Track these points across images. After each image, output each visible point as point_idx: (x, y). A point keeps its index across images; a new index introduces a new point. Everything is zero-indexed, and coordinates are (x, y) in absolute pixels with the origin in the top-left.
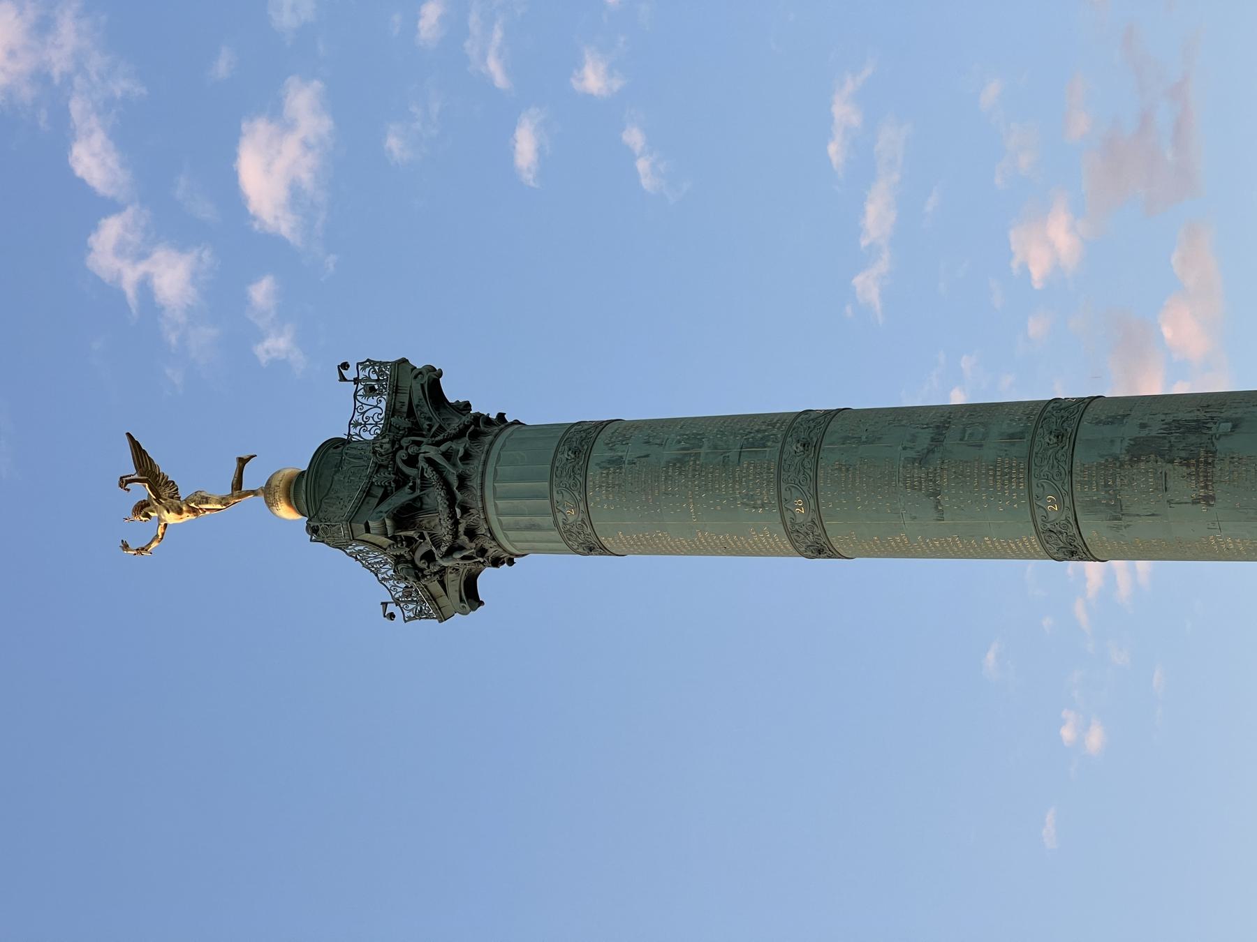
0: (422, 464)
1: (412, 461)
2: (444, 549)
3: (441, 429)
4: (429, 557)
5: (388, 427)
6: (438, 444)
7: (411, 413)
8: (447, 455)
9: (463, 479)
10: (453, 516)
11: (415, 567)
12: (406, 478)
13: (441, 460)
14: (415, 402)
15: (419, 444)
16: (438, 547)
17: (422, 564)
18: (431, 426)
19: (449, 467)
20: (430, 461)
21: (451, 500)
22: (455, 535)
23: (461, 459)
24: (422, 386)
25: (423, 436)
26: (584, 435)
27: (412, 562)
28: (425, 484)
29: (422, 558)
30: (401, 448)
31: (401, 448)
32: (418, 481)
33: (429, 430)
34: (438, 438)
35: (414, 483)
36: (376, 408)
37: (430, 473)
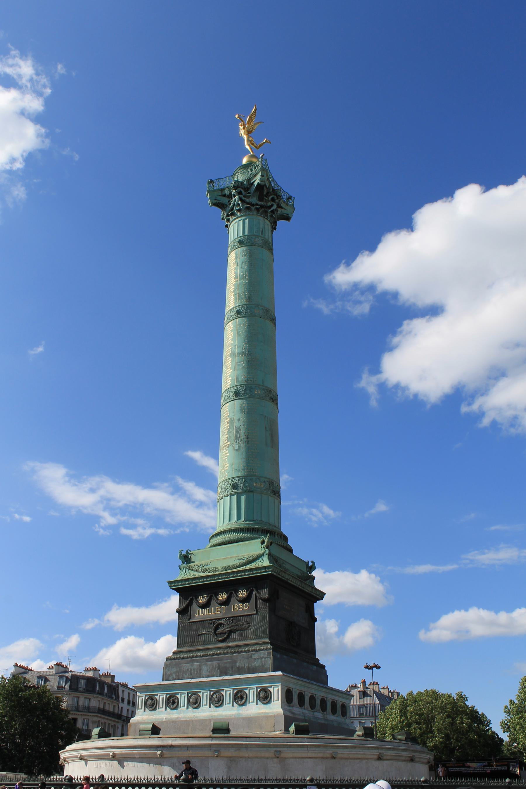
0: (272, 203)
1: (273, 200)
2: (243, 198)
8: (273, 212)
10: (257, 204)
13: (272, 209)
14: (283, 210)
16: (244, 196)
17: (238, 190)
19: (270, 210)
20: (272, 205)
22: (248, 204)
27: (239, 187)
28: (267, 201)
30: (278, 198)
36: (284, 197)
37: (269, 204)
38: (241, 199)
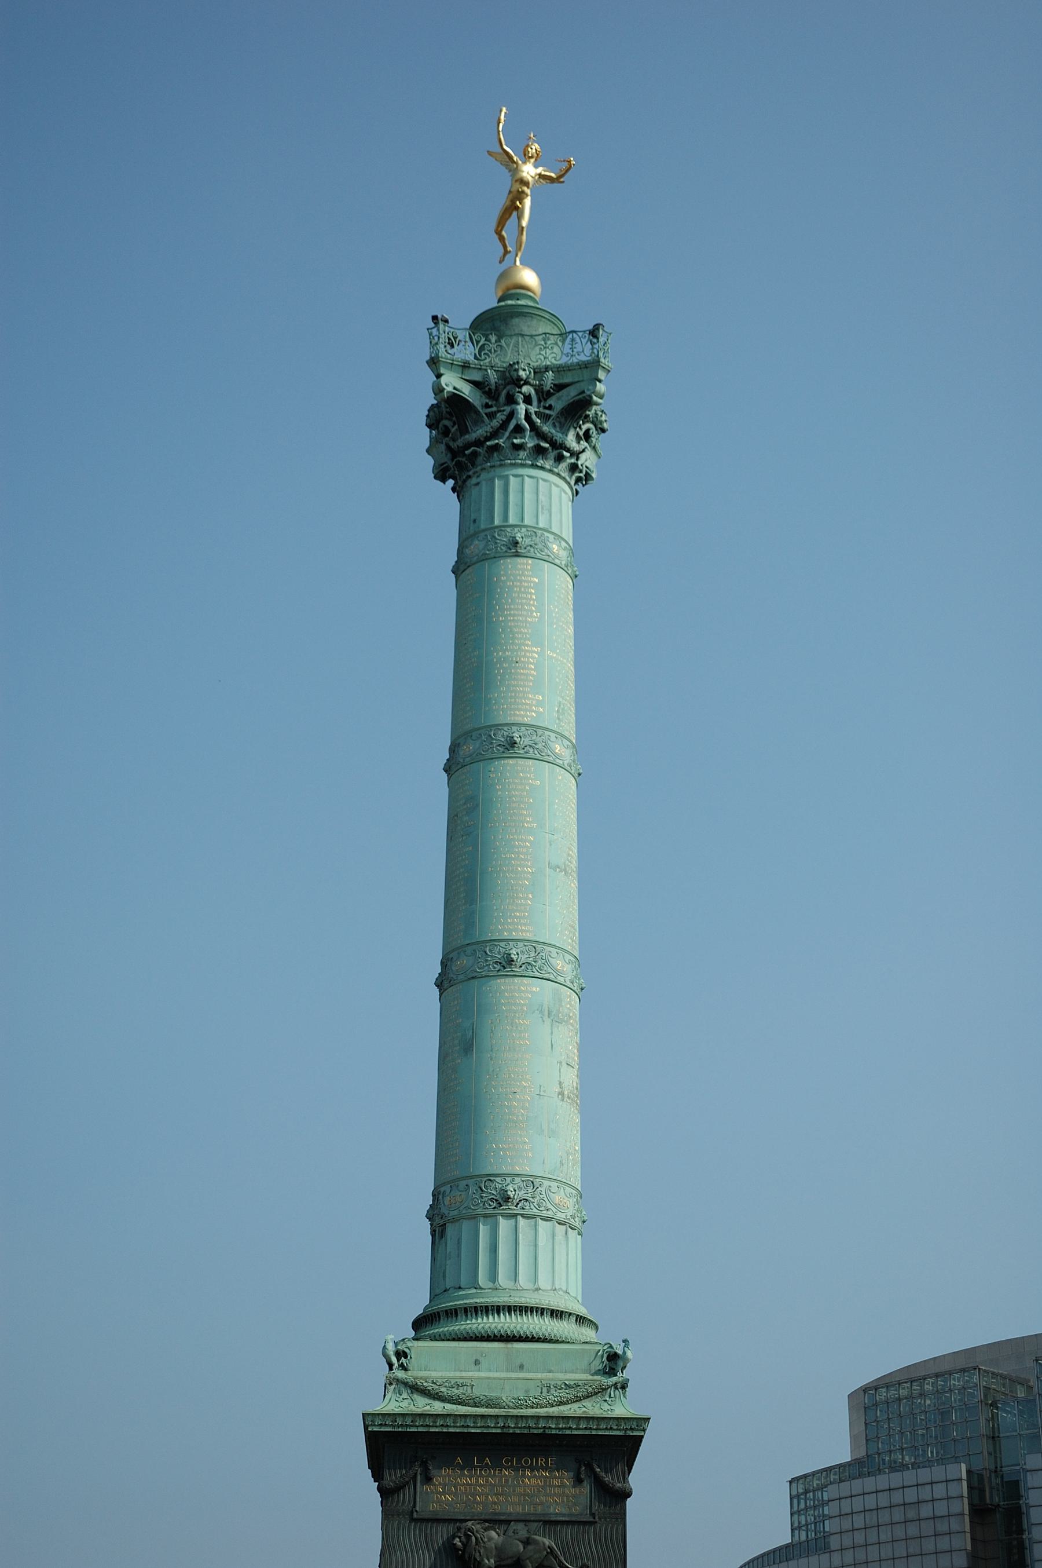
0: (508, 409)
1: (511, 400)
2: (451, 444)
3: (548, 417)
4: (446, 432)
5: (539, 372)
6: (528, 417)
7: (559, 387)
9: (496, 448)
10: (468, 446)
11: (438, 421)
12: (497, 400)
13: (512, 426)
15: (528, 400)
18: (550, 407)
19: (507, 434)
20: (512, 415)
21: (479, 443)
23: (513, 444)
24: (583, 392)
25: (539, 401)
26: (540, 546)
28: (491, 416)
29: (446, 426)
31: (520, 387)
32: (494, 409)
33: (545, 408)
34: (534, 417)
35: (491, 406)
37: (501, 417)
38: (448, 448)
